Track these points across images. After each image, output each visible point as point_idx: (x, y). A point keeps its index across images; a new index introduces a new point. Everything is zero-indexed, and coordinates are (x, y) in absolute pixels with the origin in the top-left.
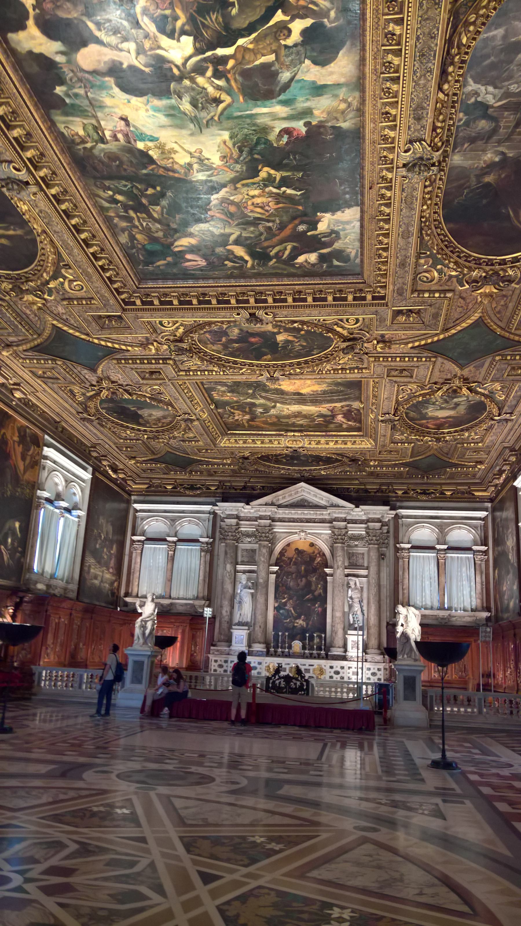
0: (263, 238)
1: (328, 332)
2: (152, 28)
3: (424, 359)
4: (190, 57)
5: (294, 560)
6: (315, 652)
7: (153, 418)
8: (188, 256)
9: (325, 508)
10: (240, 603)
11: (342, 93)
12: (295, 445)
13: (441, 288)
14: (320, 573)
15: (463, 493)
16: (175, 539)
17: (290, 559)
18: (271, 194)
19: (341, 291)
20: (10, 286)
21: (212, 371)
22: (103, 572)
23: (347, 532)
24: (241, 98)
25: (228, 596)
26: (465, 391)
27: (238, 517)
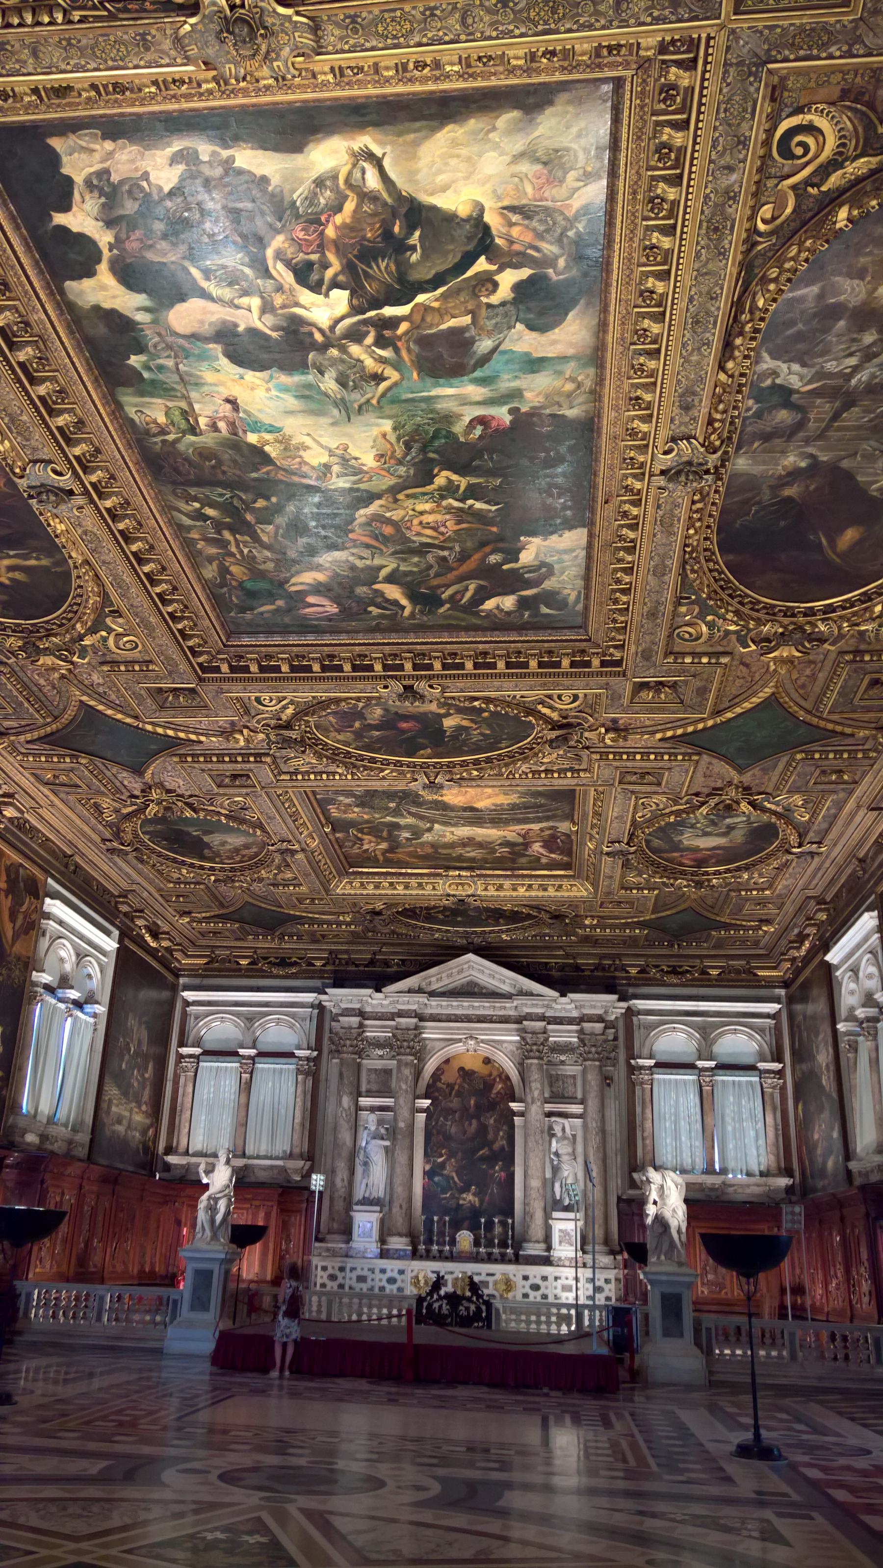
0: (432, 572)
1: (528, 714)
2: (288, 278)
3: (680, 757)
4: (342, 318)
6: (496, 1251)
7: (228, 847)
8: (311, 599)
9: (508, 996)
10: (366, 1164)
11: (569, 369)
12: (461, 892)
13: (710, 650)
15: (738, 972)
16: (253, 1052)
17: (450, 1086)
18: (449, 509)
19: (550, 653)
20: (20, 643)
21: (334, 773)
22: (131, 1111)
23: (547, 1039)
24: (415, 375)
25: (345, 1153)
26: (744, 807)
27: (361, 1014)
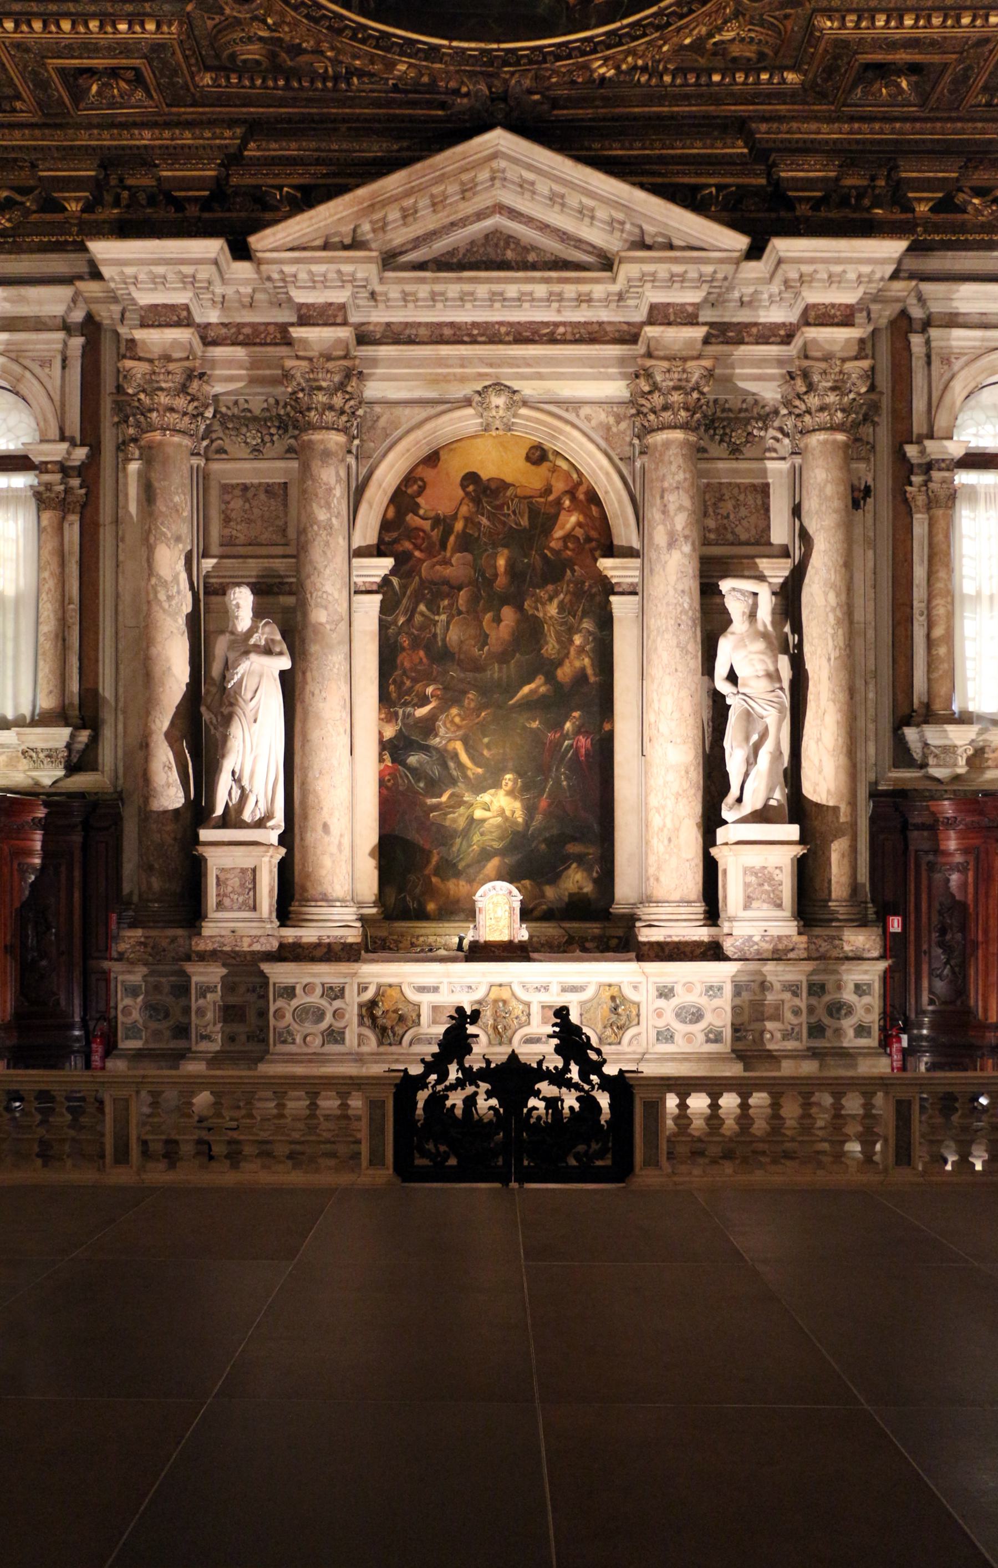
5: (459, 526)
14: (579, 583)
17: (443, 523)
